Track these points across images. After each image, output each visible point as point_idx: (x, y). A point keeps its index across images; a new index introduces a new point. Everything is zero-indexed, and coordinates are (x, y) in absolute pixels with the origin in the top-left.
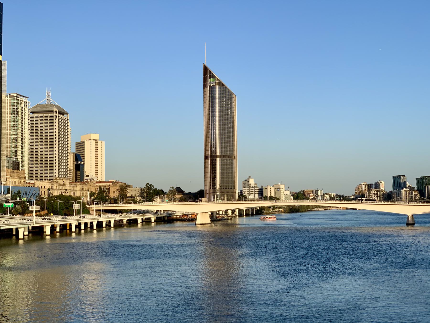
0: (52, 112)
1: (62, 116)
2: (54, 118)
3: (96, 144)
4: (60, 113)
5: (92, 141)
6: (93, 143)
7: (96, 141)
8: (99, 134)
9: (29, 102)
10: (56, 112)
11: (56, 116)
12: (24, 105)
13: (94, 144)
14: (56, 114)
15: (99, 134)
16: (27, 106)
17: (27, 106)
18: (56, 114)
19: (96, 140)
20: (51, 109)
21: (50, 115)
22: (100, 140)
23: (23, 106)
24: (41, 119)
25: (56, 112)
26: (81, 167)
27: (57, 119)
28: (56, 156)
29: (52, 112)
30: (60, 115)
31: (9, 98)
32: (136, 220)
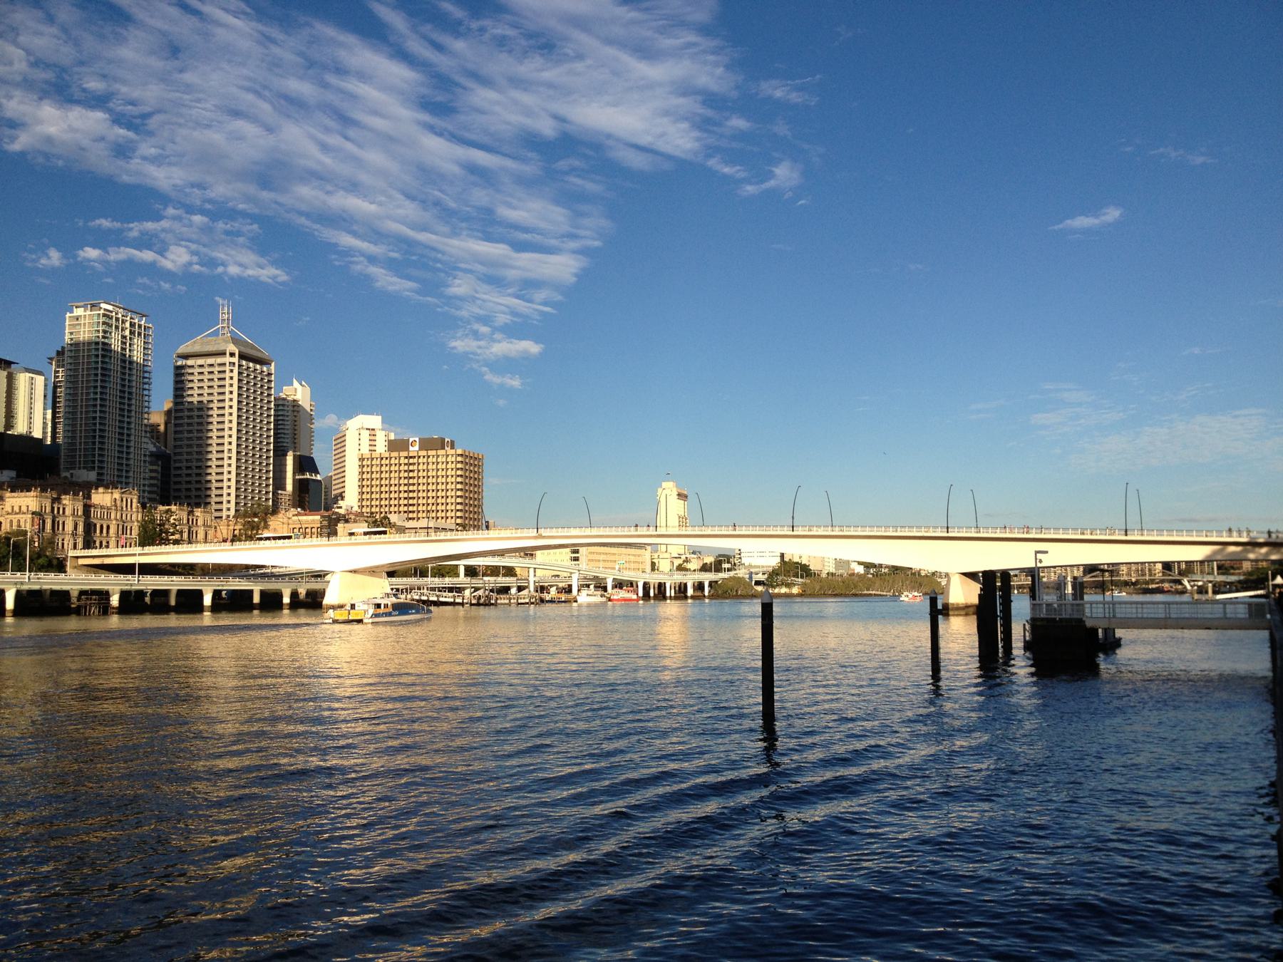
0: (223, 354)
1: (258, 367)
2: (227, 368)
3: (373, 438)
4: (242, 357)
5: (362, 432)
6: (366, 434)
7: (373, 433)
8: (379, 418)
9: (150, 325)
10: (232, 355)
12: (132, 333)
13: (368, 437)
14: (233, 360)
15: (379, 418)
16: (139, 334)
17: (139, 334)
18: (233, 360)
19: (373, 430)
20: (221, 348)
21: (220, 360)
22: (382, 430)
23: (127, 333)
24: (201, 370)
25: (232, 355)
26: (311, 486)
27: (236, 370)
30: (244, 363)
31: (88, 312)
32: (199, 594)
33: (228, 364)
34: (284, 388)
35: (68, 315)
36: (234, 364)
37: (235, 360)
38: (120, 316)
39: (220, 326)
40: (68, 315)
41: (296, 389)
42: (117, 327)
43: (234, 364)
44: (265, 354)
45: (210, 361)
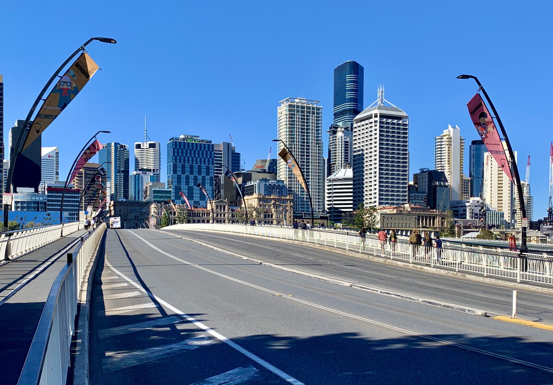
9: (321, 107)
10: (376, 116)
11: (376, 122)
12: (307, 112)
21: (371, 120)
27: (378, 124)
28: (375, 175)
29: (370, 117)
30: (384, 120)
33: (373, 122)
34: (444, 131)
35: (278, 107)
36: (377, 121)
37: (378, 119)
38: (300, 104)
39: (378, 100)
40: (278, 107)
41: (449, 131)
42: (298, 111)
43: (377, 121)
44: (404, 114)
45: (367, 122)
